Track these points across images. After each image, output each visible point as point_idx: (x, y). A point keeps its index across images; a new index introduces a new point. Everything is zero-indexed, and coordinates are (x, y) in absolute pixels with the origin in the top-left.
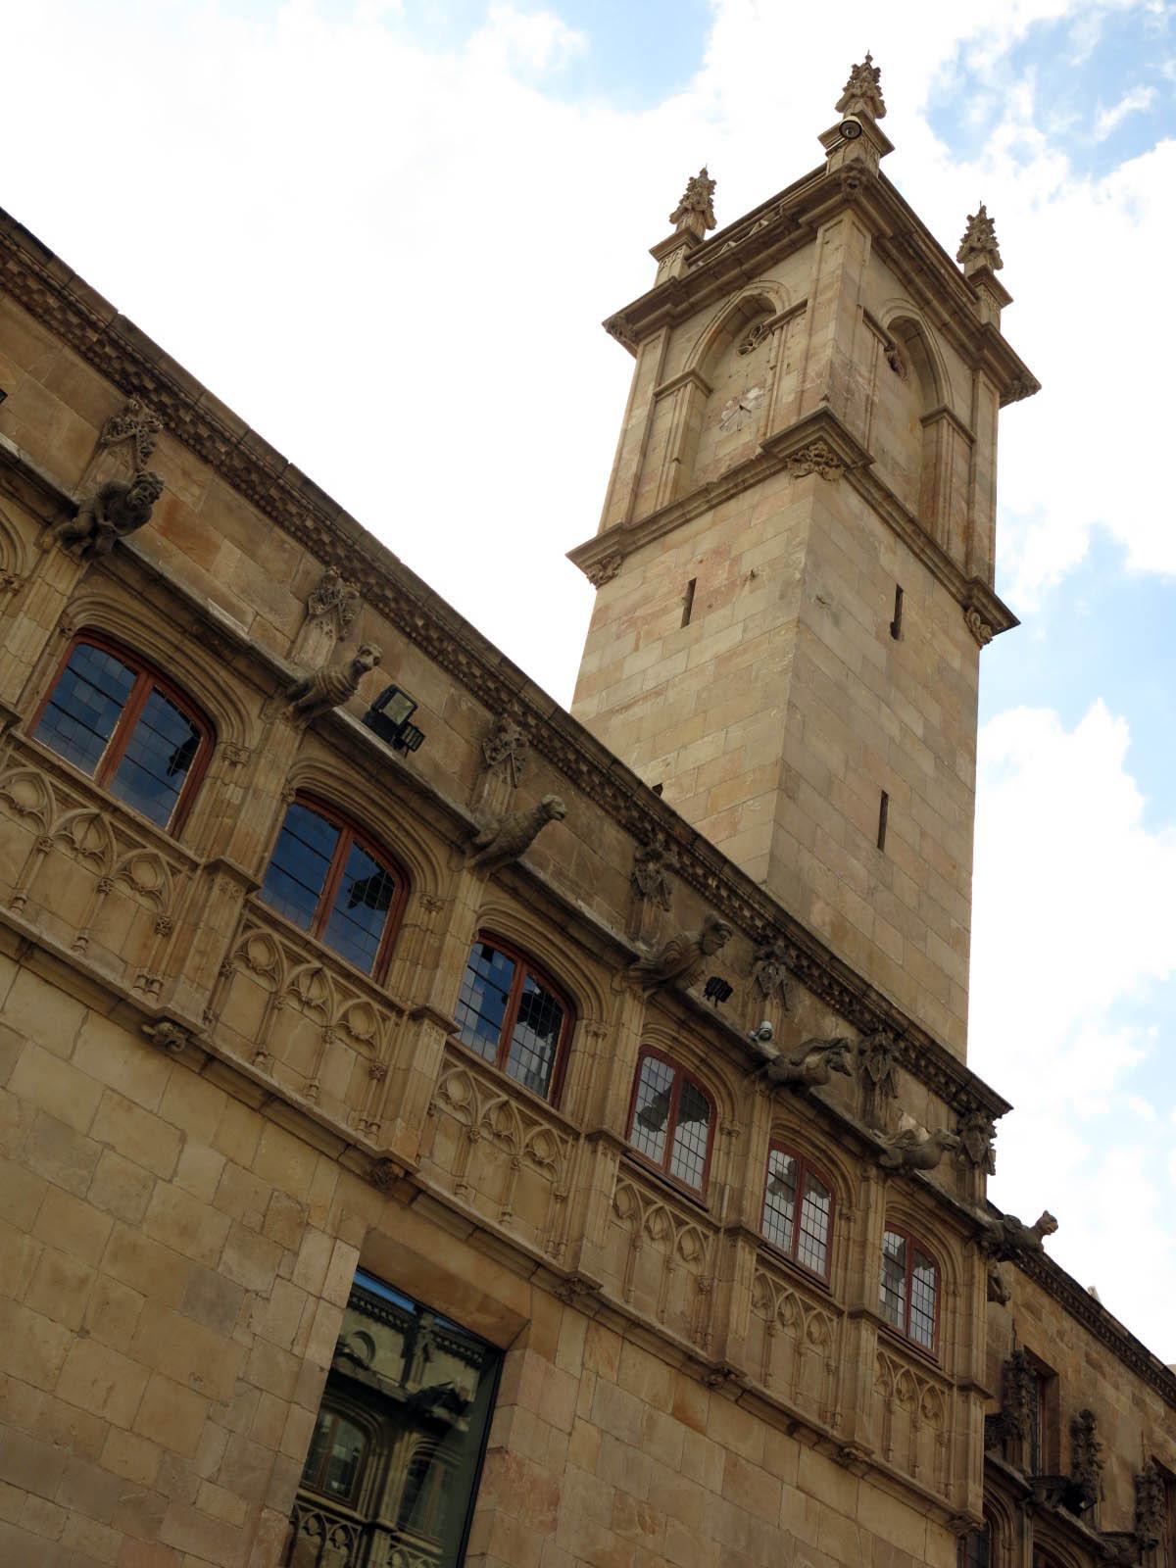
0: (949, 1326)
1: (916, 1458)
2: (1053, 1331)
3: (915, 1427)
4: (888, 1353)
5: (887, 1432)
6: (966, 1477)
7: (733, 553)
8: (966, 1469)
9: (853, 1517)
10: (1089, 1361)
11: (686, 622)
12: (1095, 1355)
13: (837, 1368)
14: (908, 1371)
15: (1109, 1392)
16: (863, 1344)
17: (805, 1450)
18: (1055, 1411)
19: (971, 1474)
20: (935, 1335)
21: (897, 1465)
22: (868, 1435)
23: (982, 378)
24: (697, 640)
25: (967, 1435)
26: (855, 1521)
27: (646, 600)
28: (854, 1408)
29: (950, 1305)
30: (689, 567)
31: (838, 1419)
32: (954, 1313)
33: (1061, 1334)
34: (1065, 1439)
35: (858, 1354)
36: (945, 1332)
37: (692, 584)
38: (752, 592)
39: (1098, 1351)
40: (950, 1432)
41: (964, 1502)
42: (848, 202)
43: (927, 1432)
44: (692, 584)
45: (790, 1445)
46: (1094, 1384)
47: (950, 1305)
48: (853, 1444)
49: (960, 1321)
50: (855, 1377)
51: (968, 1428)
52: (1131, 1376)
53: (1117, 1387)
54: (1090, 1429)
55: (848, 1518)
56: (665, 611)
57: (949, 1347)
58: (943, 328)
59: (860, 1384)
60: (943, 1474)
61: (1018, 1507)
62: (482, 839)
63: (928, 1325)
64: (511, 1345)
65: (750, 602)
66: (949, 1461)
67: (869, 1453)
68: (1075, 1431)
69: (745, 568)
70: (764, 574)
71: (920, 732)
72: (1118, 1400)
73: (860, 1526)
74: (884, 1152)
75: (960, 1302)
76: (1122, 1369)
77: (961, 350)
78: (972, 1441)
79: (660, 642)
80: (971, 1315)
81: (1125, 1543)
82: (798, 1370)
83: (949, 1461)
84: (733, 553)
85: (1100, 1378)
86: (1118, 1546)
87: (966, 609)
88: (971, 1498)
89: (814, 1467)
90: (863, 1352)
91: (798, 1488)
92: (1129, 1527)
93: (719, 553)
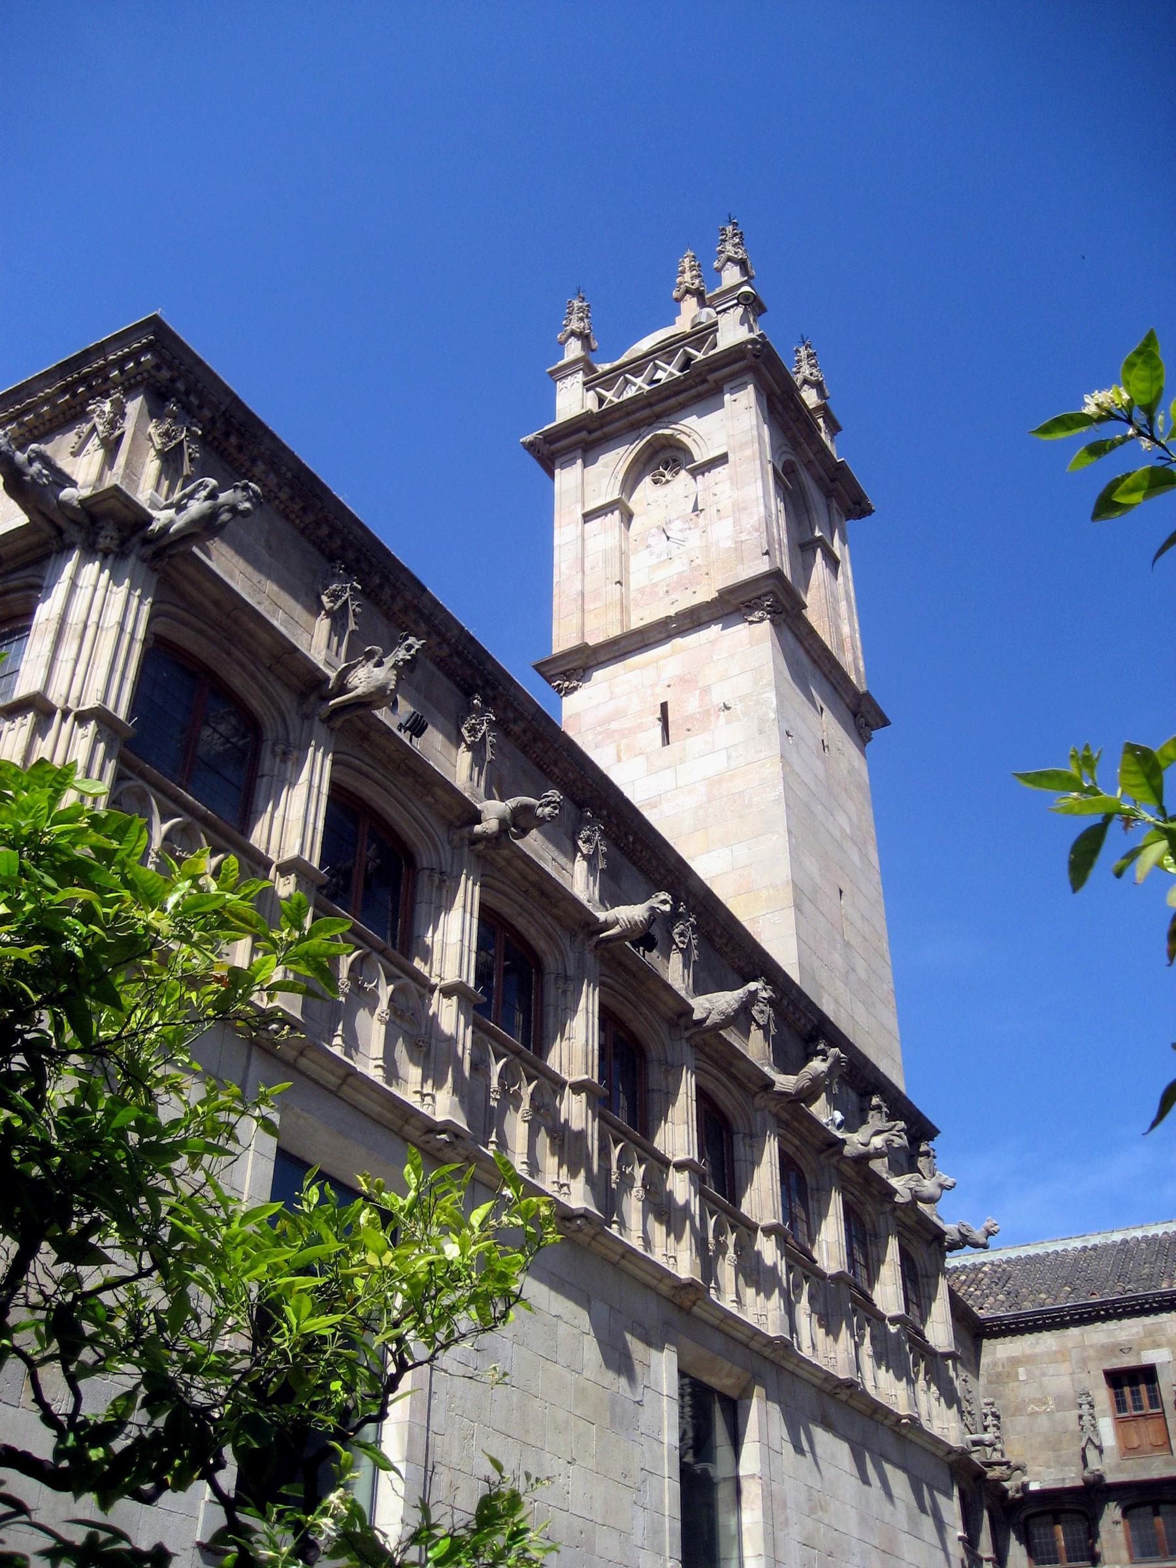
7: (700, 684)
11: (666, 739)
23: (835, 504)
24: (682, 761)
27: (618, 715)
30: (658, 690)
37: (664, 706)
38: (728, 722)
42: (749, 369)
44: (664, 706)
56: (641, 728)
58: (809, 465)
62: (697, 1016)
64: (740, 1398)
65: (726, 732)
69: (717, 699)
70: (737, 707)
71: (848, 831)
74: (895, 1192)
77: (818, 480)
79: (642, 758)
84: (700, 684)
87: (855, 715)
93: (686, 681)
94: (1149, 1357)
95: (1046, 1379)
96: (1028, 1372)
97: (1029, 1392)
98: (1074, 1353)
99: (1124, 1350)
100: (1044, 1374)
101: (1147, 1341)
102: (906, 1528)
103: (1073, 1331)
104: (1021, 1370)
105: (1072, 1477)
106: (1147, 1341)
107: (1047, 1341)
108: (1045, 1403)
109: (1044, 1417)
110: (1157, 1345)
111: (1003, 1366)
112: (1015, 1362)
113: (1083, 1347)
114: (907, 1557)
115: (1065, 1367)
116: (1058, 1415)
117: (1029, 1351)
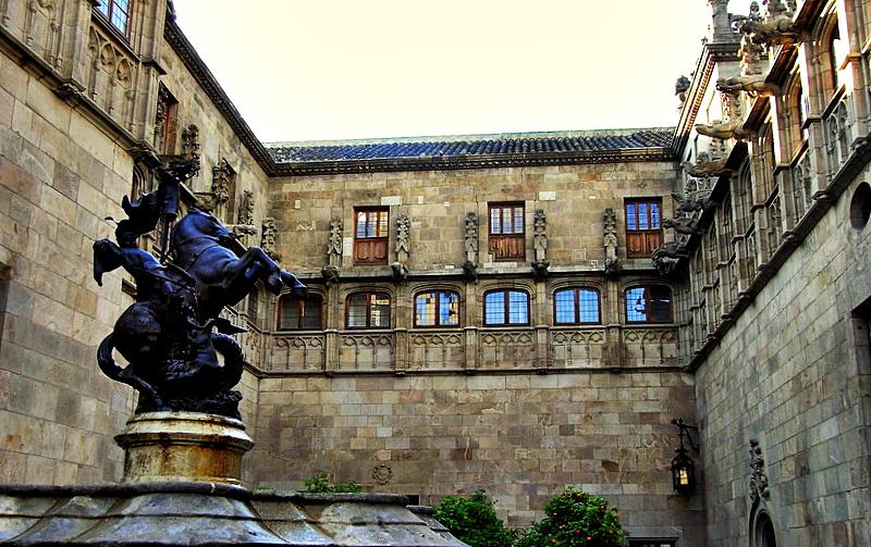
0: (139, 24)
1: (111, 102)
2: (178, 76)
3: (111, 82)
4: (96, 28)
5: (93, 82)
6: (144, 121)
8: (145, 115)
9: (66, 132)
10: (195, 98)
12: (199, 97)
13: (60, 27)
14: (109, 45)
15: (205, 118)
16: (81, 14)
17: (33, 80)
18: (175, 123)
19: (147, 118)
20: (128, 26)
21: (99, 102)
22: (81, 75)
25: (147, 94)
26: (67, 136)
28: (72, 57)
29: (140, 10)
31: (59, 62)
32: (143, 15)
33: (182, 80)
34: (179, 139)
35: (76, 20)
36: (136, 25)
39: (202, 96)
40: (135, 91)
41: (142, 135)
43: (120, 90)
45: (22, 75)
46: (197, 112)
47: (140, 10)
48: (71, 81)
49: (147, 21)
50: (74, 37)
51: (148, 89)
52: (219, 114)
53: (209, 117)
54: (194, 135)
55: (62, 132)
57: (138, 37)
59: (77, 41)
60: (128, 117)
61: (150, 172)
63: (123, 17)
66: (133, 109)
67: (81, 89)
68: (184, 136)
72: (209, 124)
73: (70, 140)
75: (148, 9)
76: (212, 106)
78: (150, 98)
80: (154, 18)
81: (209, 198)
82: (30, 21)
83: (133, 109)
85: (200, 109)
86: (204, 199)
88: (147, 133)
89: (39, 93)
90: (80, 19)
91: (26, 104)
92: (208, 190)
94: (385, 201)
95: (313, 209)
96: (302, 203)
97: (297, 216)
98: (336, 194)
99: (370, 194)
100: (313, 205)
101: (388, 191)
102: (51, 182)
103: (339, 178)
104: (297, 202)
105: (316, 273)
106: (388, 191)
107: (320, 184)
108: (310, 225)
109: (307, 234)
110: (393, 194)
111: (286, 197)
112: (295, 196)
113: (343, 191)
114: (44, 205)
115: (328, 202)
116: (316, 233)
117: (305, 190)
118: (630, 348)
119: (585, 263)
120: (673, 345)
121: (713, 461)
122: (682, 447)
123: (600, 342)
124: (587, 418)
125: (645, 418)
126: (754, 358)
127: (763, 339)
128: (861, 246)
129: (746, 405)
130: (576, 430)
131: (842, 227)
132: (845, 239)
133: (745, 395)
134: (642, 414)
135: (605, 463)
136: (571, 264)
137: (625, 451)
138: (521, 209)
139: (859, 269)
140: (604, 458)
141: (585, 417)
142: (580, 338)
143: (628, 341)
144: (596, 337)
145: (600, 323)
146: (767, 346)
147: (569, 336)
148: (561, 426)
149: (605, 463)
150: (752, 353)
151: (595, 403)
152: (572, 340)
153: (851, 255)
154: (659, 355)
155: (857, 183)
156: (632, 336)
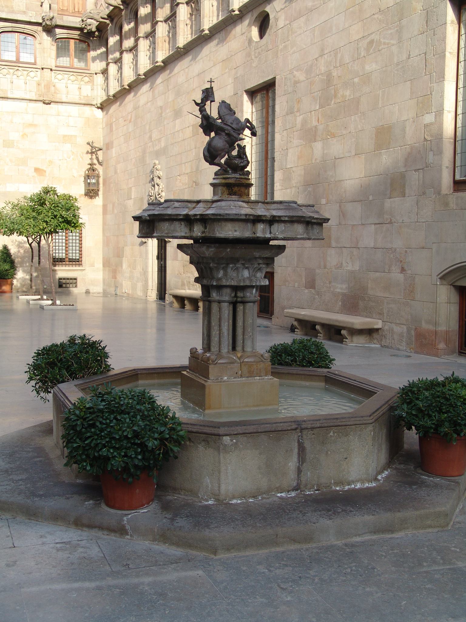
118: (58, 85)
119: (24, 13)
120: (89, 87)
121: (116, 172)
122: (92, 162)
123: (35, 79)
124: (24, 135)
125: (66, 139)
126: (161, 107)
127: (171, 96)
128: (257, 51)
129: (150, 137)
130: (15, 144)
131: (245, 35)
132: (246, 44)
133: (150, 131)
134: (65, 136)
135: (37, 170)
136: (13, 12)
137: (51, 162)
138: (458, 177)
139: (254, 65)
140: (37, 166)
141: (23, 135)
142: (19, 73)
143: (56, 81)
144: (32, 74)
145: (35, 64)
146: (173, 101)
147: (12, 71)
148: (4, 140)
149: (37, 170)
150: (160, 103)
151: (31, 125)
152: (13, 74)
153: (249, 55)
154: (78, 93)
155: (260, 10)
156: (60, 77)
